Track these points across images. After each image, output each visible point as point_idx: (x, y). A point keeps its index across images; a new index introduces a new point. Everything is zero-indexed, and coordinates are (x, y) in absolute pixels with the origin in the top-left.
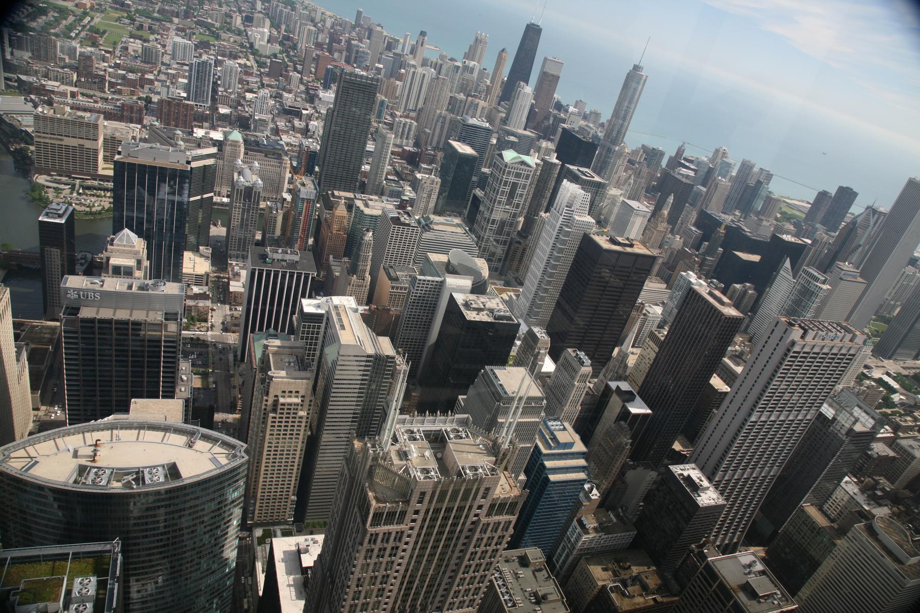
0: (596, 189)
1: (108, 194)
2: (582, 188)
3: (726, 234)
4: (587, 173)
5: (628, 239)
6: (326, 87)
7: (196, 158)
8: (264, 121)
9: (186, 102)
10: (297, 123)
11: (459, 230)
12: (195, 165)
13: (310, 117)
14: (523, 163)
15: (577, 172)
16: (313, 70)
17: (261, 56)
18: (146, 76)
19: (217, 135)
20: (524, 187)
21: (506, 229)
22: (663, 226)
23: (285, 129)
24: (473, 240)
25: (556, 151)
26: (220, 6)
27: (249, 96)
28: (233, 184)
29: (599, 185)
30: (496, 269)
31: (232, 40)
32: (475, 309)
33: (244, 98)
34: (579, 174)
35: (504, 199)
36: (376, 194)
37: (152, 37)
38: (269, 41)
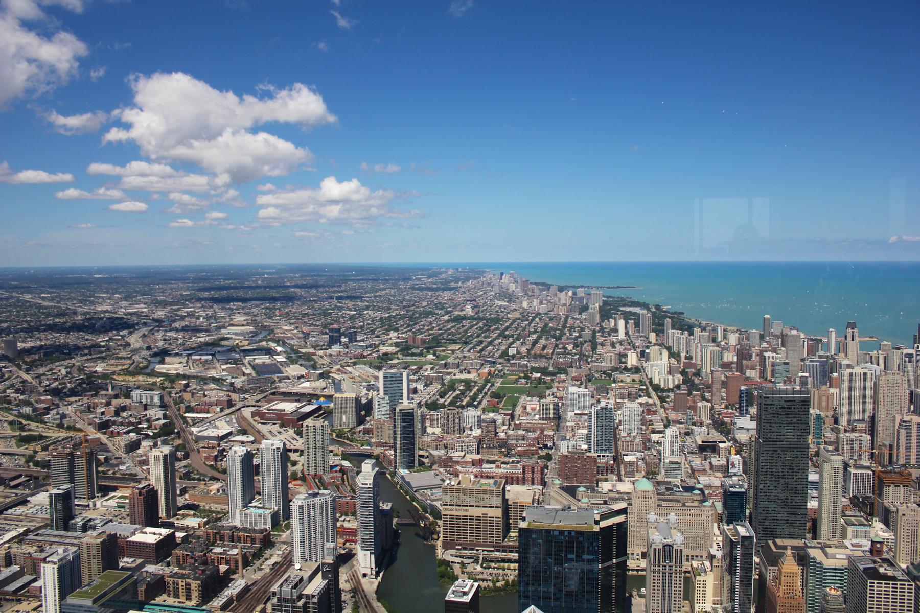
1: (512, 566)
6: (743, 411)
7: (604, 517)
9: (588, 454)
10: (715, 461)
12: (604, 524)
16: (724, 395)
17: (663, 390)
18: (545, 433)
19: (624, 487)
23: (701, 468)
26: (613, 345)
27: (655, 437)
28: (649, 545)
31: (628, 379)
33: (649, 440)
36: (834, 537)
37: (548, 392)
38: (669, 373)
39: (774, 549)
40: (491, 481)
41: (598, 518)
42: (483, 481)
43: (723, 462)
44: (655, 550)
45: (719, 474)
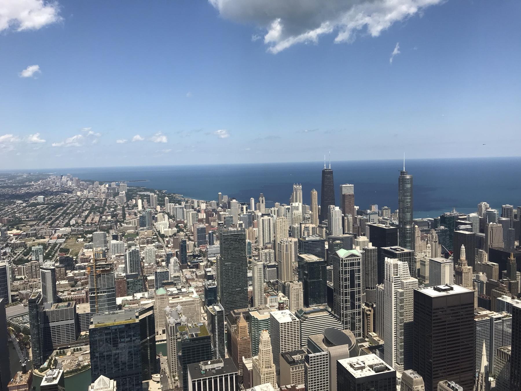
0: (409, 258)
2: (400, 260)
3: (517, 260)
4: (397, 248)
5: (447, 285)
7: (141, 313)
8: (178, 277)
11: (325, 314)
13: (206, 266)
14: (353, 255)
15: (391, 250)
20: (359, 270)
21: (357, 303)
22: (467, 268)
24: (337, 318)
25: (370, 241)
28: (167, 325)
29: (409, 254)
30: (360, 336)
32: (358, 369)
34: (393, 250)
35: (348, 283)
38: (169, 227)
39: (234, 316)
40: (66, 304)
41: (137, 314)
42: (61, 304)
43: (203, 272)
44: (171, 327)
45: (201, 280)
